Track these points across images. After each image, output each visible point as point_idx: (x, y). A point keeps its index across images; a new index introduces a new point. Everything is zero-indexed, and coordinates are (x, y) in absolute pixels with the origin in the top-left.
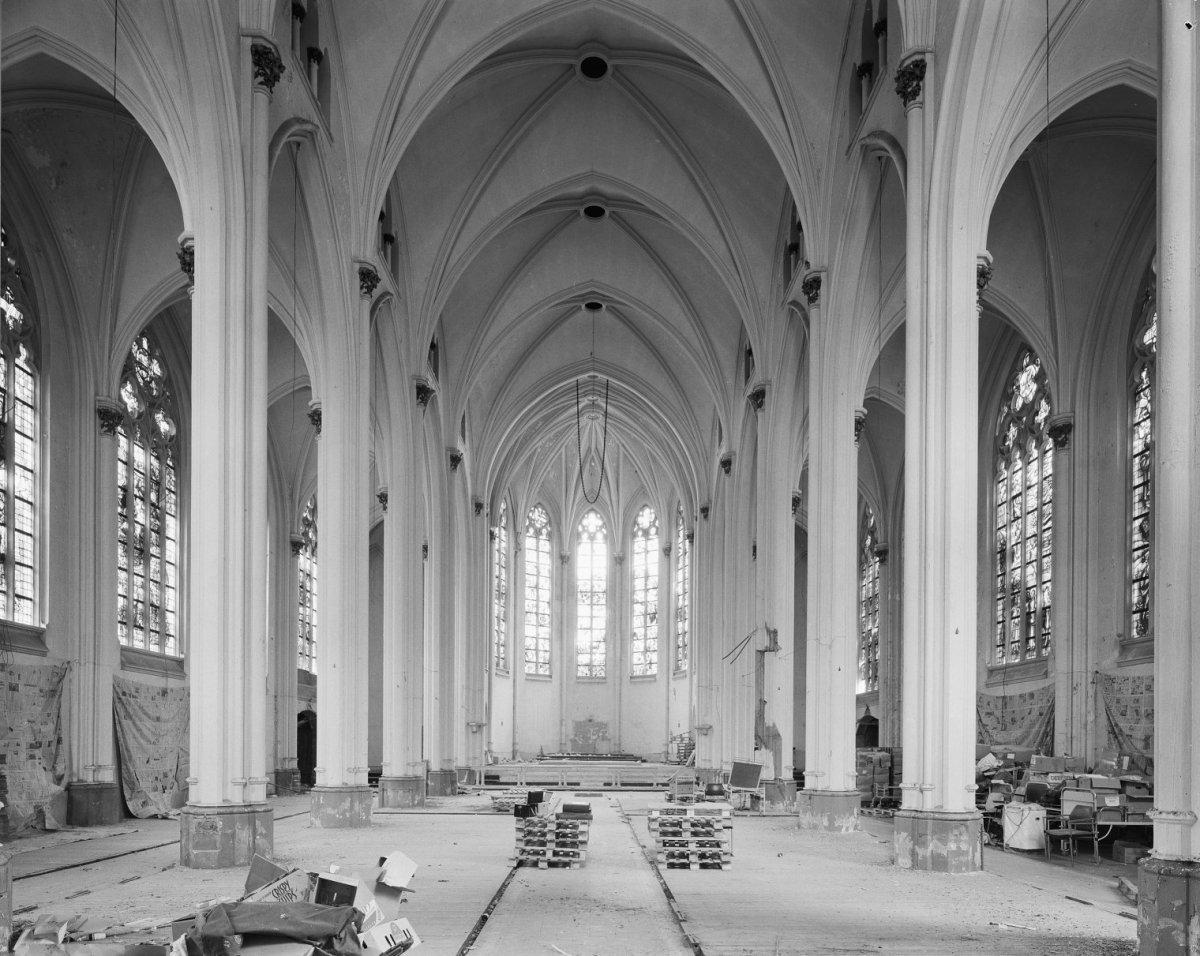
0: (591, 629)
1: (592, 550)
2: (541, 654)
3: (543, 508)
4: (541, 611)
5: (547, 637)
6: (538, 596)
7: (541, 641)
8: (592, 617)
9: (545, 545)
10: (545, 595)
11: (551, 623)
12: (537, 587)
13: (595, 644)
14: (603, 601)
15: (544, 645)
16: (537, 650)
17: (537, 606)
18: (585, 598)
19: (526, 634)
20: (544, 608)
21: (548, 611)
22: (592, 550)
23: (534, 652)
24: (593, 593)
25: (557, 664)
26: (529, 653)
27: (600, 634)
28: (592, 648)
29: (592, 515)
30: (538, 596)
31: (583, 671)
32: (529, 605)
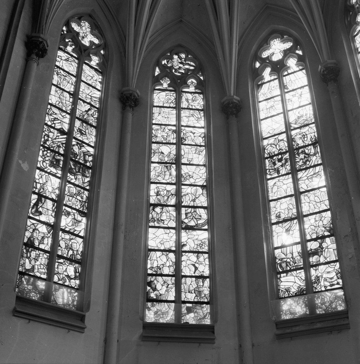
0: (300, 217)
1: (282, 86)
2: (189, 284)
3: (187, 53)
4: (186, 201)
5: (206, 249)
6: (179, 176)
7: (188, 260)
8: (297, 194)
9: (193, 99)
10: (198, 175)
11: (210, 221)
12: (178, 162)
13: (313, 246)
14: (316, 159)
15: (196, 265)
16: (178, 276)
17: (178, 194)
18: (279, 164)
19: (152, 244)
20: (196, 196)
21: (203, 201)
22: (282, 86)
23: (171, 281)
24: (293, 150)
25: (228, 301)
26: (159, 282)
27: (317, 225)
28: (306, 254)
29: (291, 59)
30: (179, 176)
31: (292, 308)
32: (160, 188)
